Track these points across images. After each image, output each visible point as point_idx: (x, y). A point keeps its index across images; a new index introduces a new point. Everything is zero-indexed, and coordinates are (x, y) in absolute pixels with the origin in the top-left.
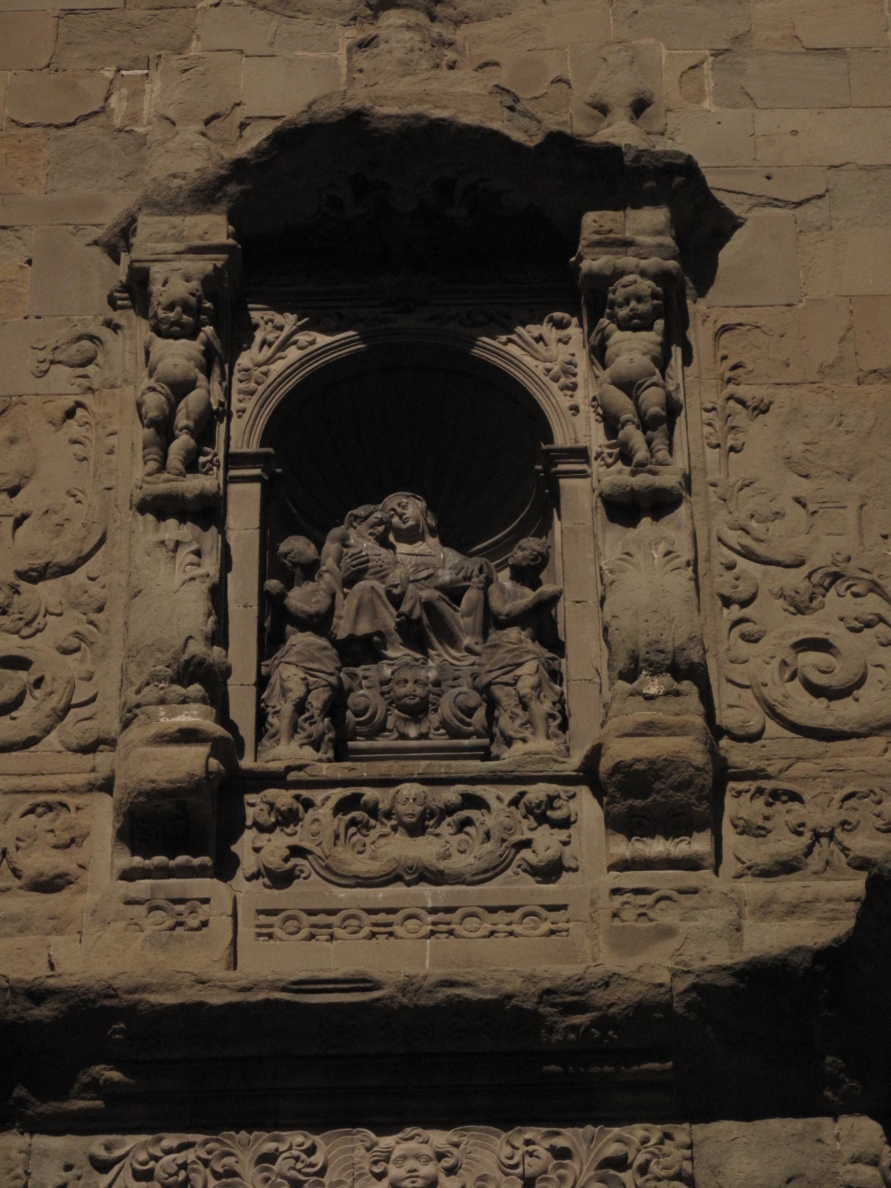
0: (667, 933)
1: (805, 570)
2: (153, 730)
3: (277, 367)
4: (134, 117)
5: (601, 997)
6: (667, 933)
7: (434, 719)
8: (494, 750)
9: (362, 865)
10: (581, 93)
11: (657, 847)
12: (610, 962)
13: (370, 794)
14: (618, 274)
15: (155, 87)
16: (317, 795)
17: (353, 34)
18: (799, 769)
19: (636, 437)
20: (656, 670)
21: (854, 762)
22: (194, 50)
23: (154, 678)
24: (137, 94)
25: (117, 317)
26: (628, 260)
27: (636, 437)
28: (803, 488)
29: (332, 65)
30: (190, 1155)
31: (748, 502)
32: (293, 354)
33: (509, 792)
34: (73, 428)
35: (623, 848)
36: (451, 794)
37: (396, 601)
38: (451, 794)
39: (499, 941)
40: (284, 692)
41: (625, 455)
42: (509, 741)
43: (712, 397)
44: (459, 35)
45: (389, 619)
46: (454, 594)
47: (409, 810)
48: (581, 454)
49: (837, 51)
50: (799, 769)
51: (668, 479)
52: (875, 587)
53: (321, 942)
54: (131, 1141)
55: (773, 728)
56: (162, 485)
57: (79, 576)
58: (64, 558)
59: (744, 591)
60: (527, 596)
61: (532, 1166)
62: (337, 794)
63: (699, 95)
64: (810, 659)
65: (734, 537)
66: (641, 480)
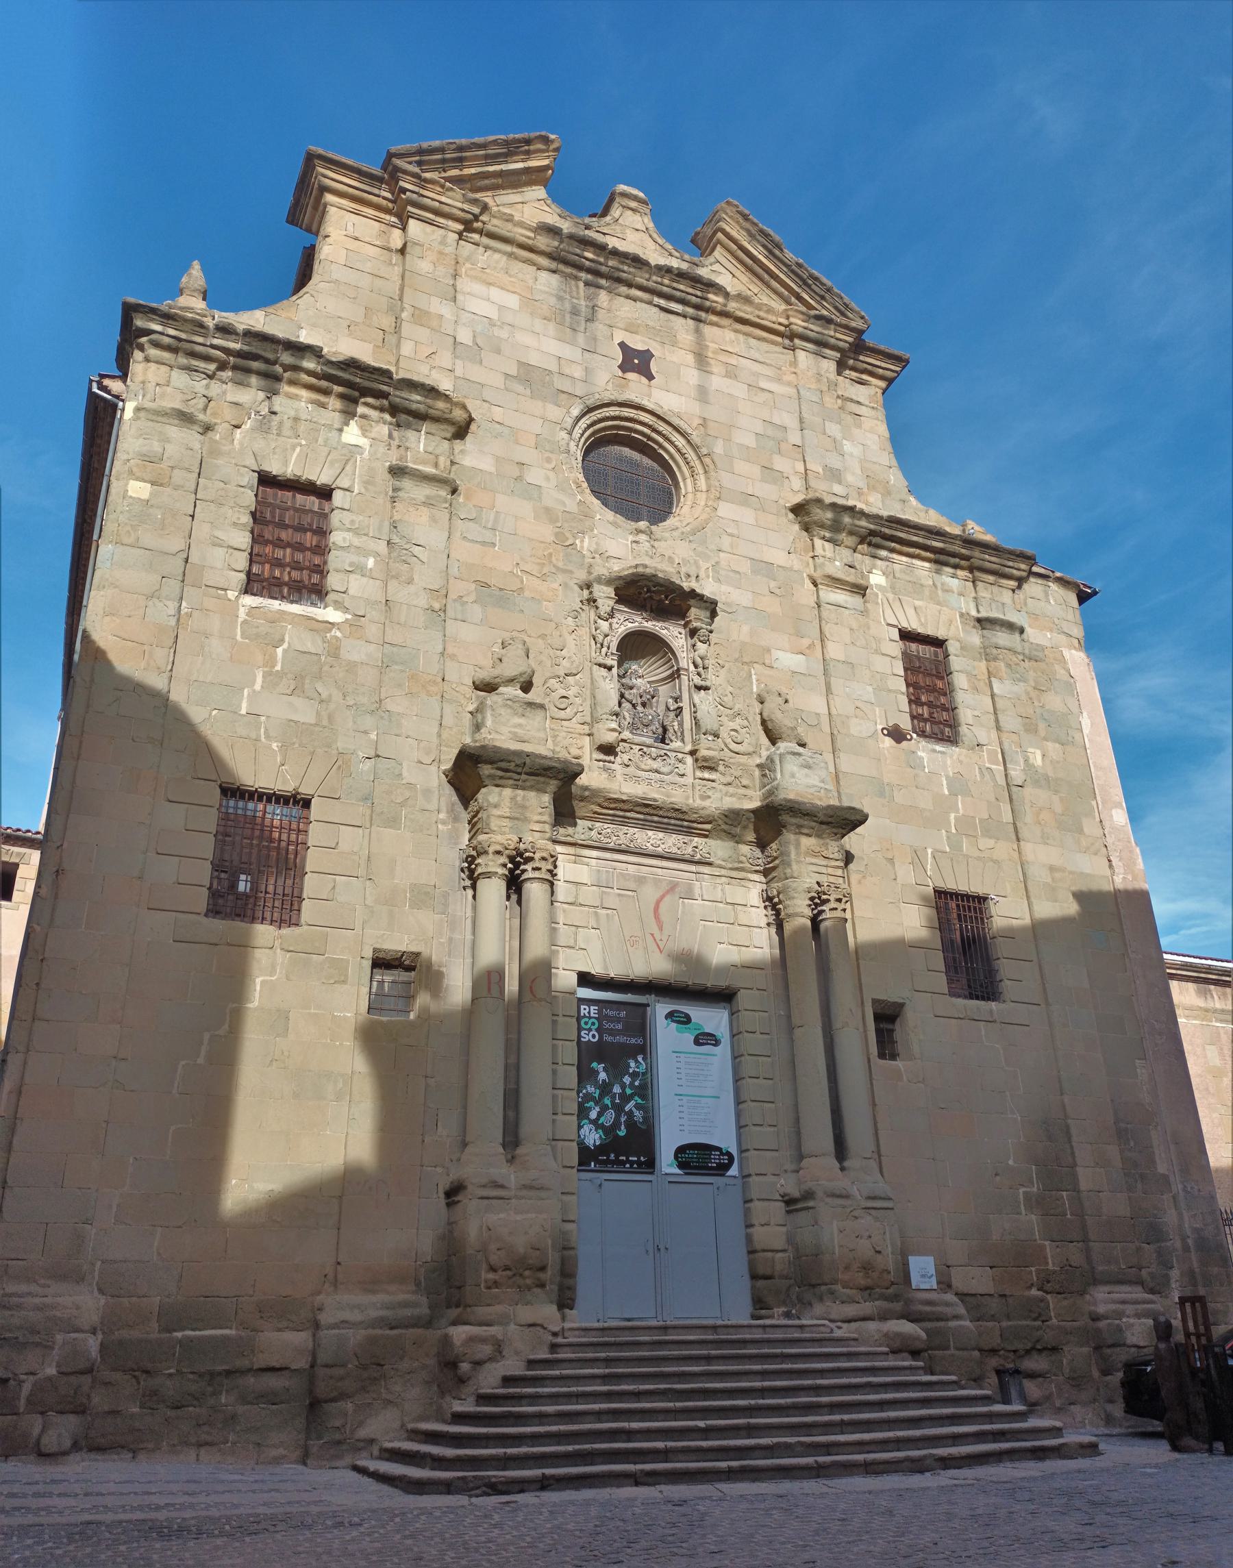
0: (709, 797)
1: (732, 711)
2: (606, 727)
3: (620, 630)
4: (582, 547)
5: (701, 812)
6: (709, 797)
7: (650, 728)
8: (667, 742)
9: (643, 767)
10: (683, 570)
11: (706, 775)
12: (698, 803)
13: (645, 749)
14: (702, 628)
15: (586, 540)
16: (634, 747)
17: (631, 538)
18: (731, 760)
19: (700, 670)
20: (711, 734)
21: (741, 760)
22: (596, 531)
23: (606, 714)
24: (582, 541)
25: (584, 607)
26: (704, 626)
27: (700, 670)
28: (731, 689)
29: (627, 545)
30: (609, 830)
31: (720, 691)
32: (623, 628)
33: (674, 754)
34: (573, 636)
35: (699, 774)
36: (662, 752)
37: (641, 697)
38: (662, 752)
39: (674, 792)
40: (624, 718)
41: (699, 674)
42: (672, 741)
43: (714, 662)
44: (656, 544)
45: (639, 701)
46: (653, 697)
47: (654, 755)
48: (687, 670)
49: (738, 572)
50: (731, 760)
51: (708, 683)
52: (746, 719)
53: (637, 785)
54: (598, 824)
55: (726, 749)
56: (600, 660)
57: (577, 677)
58: (575, 672)
59: (720, 714)
60: (676, 706)
61: (679, 845)
62: (639, 747)
63: (708, 577)
64: (733, 733)
65: (718, 699)
66: (703, 683)
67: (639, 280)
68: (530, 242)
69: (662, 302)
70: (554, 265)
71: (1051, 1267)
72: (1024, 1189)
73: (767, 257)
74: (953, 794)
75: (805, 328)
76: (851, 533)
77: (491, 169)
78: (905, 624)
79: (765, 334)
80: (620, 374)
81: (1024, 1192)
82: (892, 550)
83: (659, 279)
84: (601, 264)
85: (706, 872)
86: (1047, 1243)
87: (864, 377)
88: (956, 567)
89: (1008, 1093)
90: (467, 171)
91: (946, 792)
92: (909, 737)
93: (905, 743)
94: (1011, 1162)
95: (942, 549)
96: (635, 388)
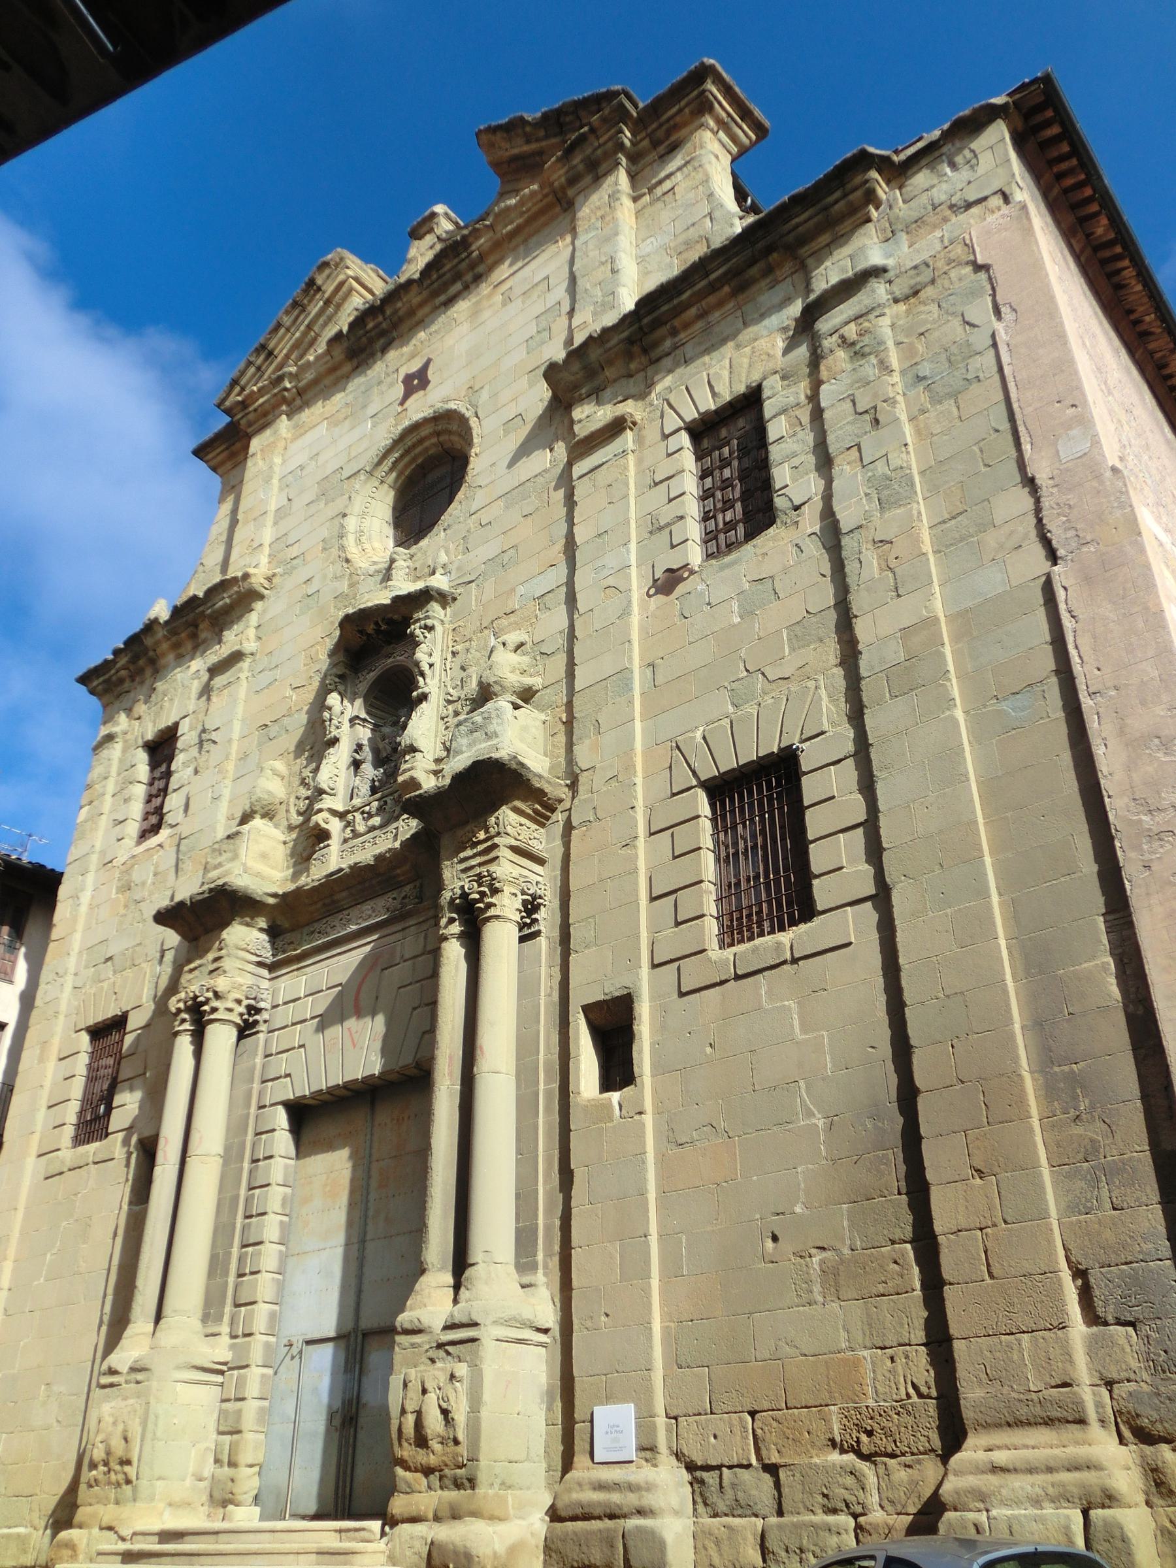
67: (416, 300)
68: (329, 365)
69: (442, 298)
70: (355, 362)
71: (871, 1402)
72: (824, 1255)
73: (528, 142)
74: (747, 613)
75: (567, 172)
76: (610, 363)
77: (298, 335)
78: (691, 414)
79: (543, 219)
80: (400, 409)
81: (823, 1262)
82: (674, 332)
83: (429, 282)
84: (380, 323)
85: (411, 923)
86: (866, 1353)
87: (673, 139)
88: (769, 271)
89: (802, 1084)
90: (279, 358)
91: (737, 620)
92: (686, 575)
93: (680, 589)
94: (798, 1209)
95: (725, 274)
96: (420, 407)
